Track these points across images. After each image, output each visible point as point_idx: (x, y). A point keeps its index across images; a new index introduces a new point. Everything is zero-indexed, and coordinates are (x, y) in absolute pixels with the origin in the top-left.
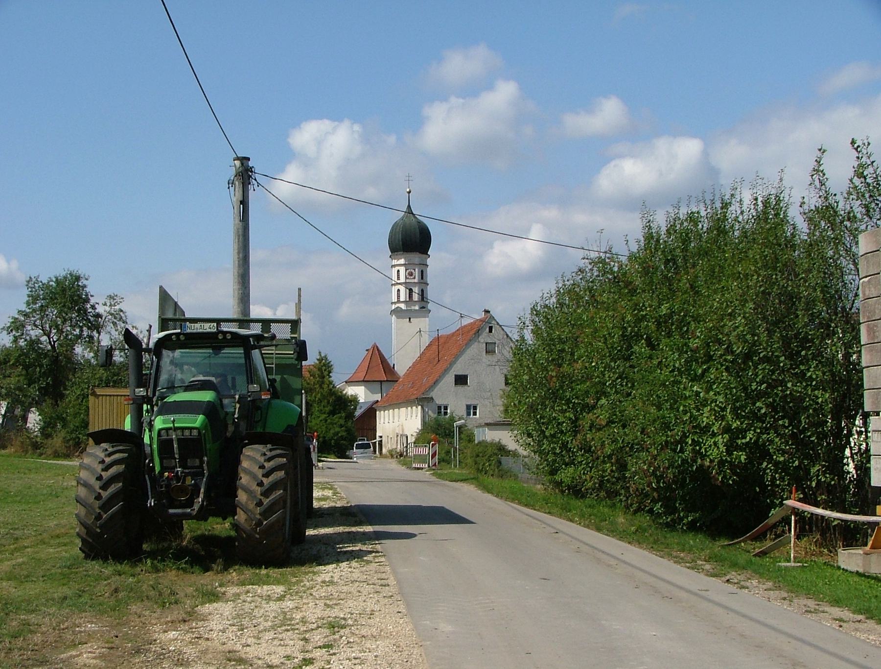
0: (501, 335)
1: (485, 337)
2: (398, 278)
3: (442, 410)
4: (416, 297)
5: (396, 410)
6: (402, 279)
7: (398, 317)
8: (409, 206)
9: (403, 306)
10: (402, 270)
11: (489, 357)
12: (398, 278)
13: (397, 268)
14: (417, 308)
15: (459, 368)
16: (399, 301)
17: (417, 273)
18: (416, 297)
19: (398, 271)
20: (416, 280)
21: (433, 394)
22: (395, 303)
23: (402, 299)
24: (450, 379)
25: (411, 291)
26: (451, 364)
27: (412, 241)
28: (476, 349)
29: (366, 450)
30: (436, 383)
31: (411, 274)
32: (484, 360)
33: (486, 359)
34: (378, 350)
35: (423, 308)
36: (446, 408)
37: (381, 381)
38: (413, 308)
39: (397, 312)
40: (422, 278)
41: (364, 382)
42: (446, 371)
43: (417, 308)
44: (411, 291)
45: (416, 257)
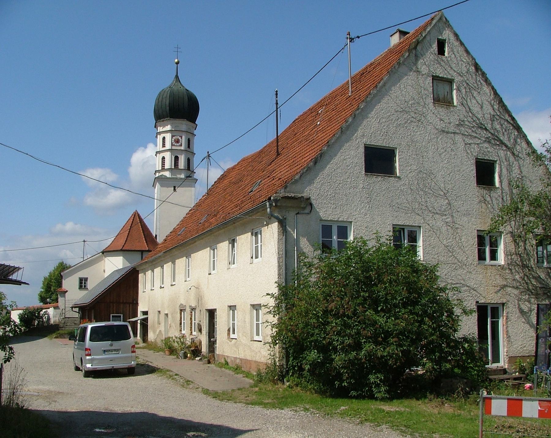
0: (464, 66)
1: (428, 63)
2: (164, 145)
3: (331, 236)
4: (182, 164)
5: (181, 262)
6: (168, 146)
7: (162, 186)
8: (177, 77)
9: (167, 174)
10: (168, 136)
11: (442, 111)
12: (164, 145)
13: (163, 135)
14: (183, 176)
15: (374, 130)
16: (163, 169)
17: (184, 141)
18: (182, 164)
19: (164, 139)
20: (182, 148)
21: (313, 191)
22: (159, 171)
23: (167, 166)
24: (352, 155)
25: (177, 158)
26: (358, 116)
27: (180, 108)
28: (411, 88)
29: (117, 344)
30: (319, 160)
31: (177, 141)
32: (431, 117)
33: (435, 115)
35: (189, 177)
36: (343, 232)
37: (142, 252)
38: (178, 176)
39: (161, 180)
40: (189, 147)
41: (123, 251)
42: (345, 132)
43: (183, 176)
44: (177, 158)
45: (184, 124)
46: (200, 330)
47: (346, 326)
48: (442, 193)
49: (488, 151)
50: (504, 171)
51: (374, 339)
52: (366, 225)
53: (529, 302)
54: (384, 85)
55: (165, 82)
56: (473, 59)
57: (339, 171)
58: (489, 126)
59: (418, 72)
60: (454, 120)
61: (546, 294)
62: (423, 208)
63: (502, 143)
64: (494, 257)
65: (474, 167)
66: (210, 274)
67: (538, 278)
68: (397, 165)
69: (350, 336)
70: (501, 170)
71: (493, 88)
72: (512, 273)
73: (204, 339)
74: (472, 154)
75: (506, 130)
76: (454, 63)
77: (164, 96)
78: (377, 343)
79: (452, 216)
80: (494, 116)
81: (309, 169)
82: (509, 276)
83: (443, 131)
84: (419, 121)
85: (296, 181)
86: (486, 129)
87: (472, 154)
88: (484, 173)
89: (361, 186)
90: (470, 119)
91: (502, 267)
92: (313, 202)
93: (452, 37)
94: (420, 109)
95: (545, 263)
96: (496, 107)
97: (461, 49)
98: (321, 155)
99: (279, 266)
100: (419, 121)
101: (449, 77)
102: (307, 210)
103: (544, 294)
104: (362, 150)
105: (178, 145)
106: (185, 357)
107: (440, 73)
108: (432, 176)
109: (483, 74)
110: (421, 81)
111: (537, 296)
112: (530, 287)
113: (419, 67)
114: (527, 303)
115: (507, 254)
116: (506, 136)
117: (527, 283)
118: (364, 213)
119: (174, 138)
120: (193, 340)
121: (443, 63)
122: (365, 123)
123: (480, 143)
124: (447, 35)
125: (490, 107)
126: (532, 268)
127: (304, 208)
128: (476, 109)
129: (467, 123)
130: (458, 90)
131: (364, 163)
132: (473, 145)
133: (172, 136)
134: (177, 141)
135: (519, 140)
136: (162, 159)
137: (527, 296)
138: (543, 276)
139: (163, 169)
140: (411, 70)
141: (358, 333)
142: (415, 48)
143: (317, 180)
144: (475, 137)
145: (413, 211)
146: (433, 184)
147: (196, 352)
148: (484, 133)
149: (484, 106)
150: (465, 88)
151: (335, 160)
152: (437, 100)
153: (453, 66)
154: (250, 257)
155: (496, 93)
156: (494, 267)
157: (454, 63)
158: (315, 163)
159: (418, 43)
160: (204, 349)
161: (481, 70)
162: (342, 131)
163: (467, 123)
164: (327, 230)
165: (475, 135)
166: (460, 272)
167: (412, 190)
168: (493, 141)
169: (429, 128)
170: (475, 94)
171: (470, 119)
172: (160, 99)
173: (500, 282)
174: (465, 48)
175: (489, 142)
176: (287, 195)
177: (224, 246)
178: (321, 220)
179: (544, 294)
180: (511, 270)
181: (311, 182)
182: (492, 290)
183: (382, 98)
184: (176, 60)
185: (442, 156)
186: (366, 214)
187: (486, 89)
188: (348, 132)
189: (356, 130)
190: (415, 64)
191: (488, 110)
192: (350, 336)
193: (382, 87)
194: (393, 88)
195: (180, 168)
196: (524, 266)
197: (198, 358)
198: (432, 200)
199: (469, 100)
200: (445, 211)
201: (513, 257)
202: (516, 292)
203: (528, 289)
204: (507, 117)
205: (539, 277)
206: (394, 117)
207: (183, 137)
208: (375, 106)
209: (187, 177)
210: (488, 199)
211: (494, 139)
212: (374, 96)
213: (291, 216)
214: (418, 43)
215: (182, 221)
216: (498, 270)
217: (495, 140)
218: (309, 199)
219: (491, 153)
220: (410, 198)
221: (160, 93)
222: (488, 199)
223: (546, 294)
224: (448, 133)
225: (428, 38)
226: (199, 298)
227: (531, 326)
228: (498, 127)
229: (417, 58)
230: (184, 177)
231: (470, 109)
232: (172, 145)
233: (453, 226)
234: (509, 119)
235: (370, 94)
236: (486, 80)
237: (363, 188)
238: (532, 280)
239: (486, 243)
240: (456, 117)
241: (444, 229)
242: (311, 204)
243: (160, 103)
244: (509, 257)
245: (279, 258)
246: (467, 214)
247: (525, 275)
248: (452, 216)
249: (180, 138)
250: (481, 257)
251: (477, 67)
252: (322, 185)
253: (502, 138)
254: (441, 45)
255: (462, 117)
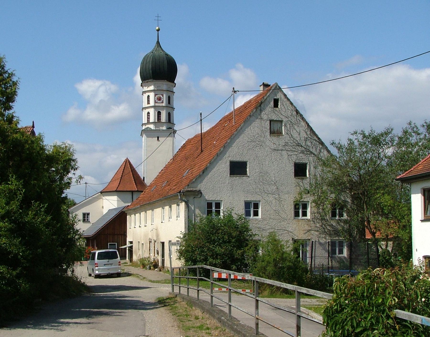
0: (289, 111)
1: (269, 112)
2: (148, 103)
3: (213, 207)
4: (164, 118)
5: (149, 212)
6: (152, 103)
7: (148, 136)
8: (158, 43)
9: (152, 127)
10: (152, 95)
11: (275, 139)
12: (148, 103)
13: (147, 94)
14: (164, 128)
15: (235, 153)
16: (148, 122)
17: (165, 98)
18: (164, 118)
19: (148, 97)
20: (164, 104)
21: (201, 186)
22: (145, 124)
23: (152, 120)
24: (223, 167)
25: (159, 113)
26: (226, 147)
27: (161, 71)
28: (258, 128)
29: (111, 261)
30: (205, 171)
31: (159, 99)
32: (268, 143)
33: (271, 142)
34: (129, 161)
35: (170, 128)
36: (218, 205)
37: (132, 192)
38: (161, 128)
39: (147, 132)
40: (169, 103)
41: (117, 192)
42: (219, 156)
43: (164, 128)
44: (159, 113)
45: (164, 85)
46: (158, 254)
47: (202, 251)
48: (273, 183)
49: (302, 158)
50: (312, 168)
51: (212, 256)
52: (230, 202)
53: (325, 238)
54: (241, 128)
55: (147, 48)
56: (295, 107)
57: (216, 175)
58: (303, 144)
59: (261, 119)
60: (282, 142)
61: (336, 234)
62: (262, 191)
63: (312, 153)
64: (305, 214)
65: (293, 168)
66: (162, 222)
67: (331, 226)
68: (248, 170)
69: (203, 255)
70: (310, 168)
71: (307, 123)
72: (315, 223)
73: (160, 258)
74: (292, 161)
75: (314, 145)
76: (283, 112)
77: (148, 60)
78: (213, 259)
79: (279, 195)
80: (307, 138)
81: (200, 176)
82: (313, 225)
83: (275, 150)
84: (261, 145)
85: (194, 182)
86: (301, 146)
87: (292, 161)
88: (300, 170)
89: (228, 182)
90: (292, 142)
91: (309, 220)
92: (202, 192)
93: (283, 97)
94: (262, 139)
95: (337, 217)
96: (308, 133)
97: (288, 103)
98: (206, 168)
99: (185, 223)
100: (261, 145)
101: (280, 119)
102: (199, 196)
103: (335, 234)
104: (228, 164)
105: (160, 102)
106: (150, 269)
107: (274, 118)
108: (268, 174)
109: (301, 115)
110: (263, 124)
111: (330, 235)
112: (326, 231)
113: (262, 116)
114: (323, 239)
115: (311, 213)
116: (314, 149)
117: (324, 228)
118: (229, 196)
119: (157, 96)
120: (154, 260)
121: (276, 112)
122: (230, 149)
123: (298, 154)
124: (279, 96)
125: (304, 133)
126: (328, 220)
127: (197, 195)
128: (295, 135)
129: (290, 144)
130: (285, 126)
131: (229, 171)
132: (293, 156)
133: (155, 95)
134: (159, 99)
135: (322, 150)
136: (148, 114)
137: (324, 235)
138: (334, 224)
139: (148, 122)
140: (257, 119)
141: (207, 254)
142: (260, 106)
143: (205, 181)
144: (295, 151)
145: (256, 193)
146: (268, 178)
147: (156, 266)
148: (300, 149)
149: (301, 133)
150: (290, 124)
151: (214, 170)
152: (272, 133)
153: (283, 113)
154: (176, 216)
155: (308, 125)
156: (303, 221)
157: (283, 112)
158: (203, 173)
159: (262, 103)
160: (160, 264)
161: (300, 113)
162: (217, 156)
163: (290, 144)
164: (209, 205)
165: (294, 150)
166: (283, 223)
167: (255, 182)
168: (305, 152)
169: (267, 149)
170: (296, 127)
171: (292, 142)
172: (145, 63)
173: (307, 228)
174: (290, 101)
175: (303, 153)
176: (189, 189)
177: (167, 208)
178: (206, 200)
179: (335, 234)
180: (314, 221)
181: (201, 182)
182: (302, 232)
183: (240, 136)
184: (157, 28)
185: (274, 163)
186: (230, 196)
187: (303, 123)
188: (221, 156)
189: (226, 154)
190: (260, 114)
191: (303, 135)
192: (203, 255)
193: (240, 130)
194: (246, 130)
195: (162, 121)
196: (322, 219)
197: (156, 269)
198: (267, 187)
199: (291, 131)
200: (275, 192)
201: (315, 215)
202: (317, 233)
203: (325, 232)
204: (315, 138)
205: (332, 225)
206: (247, 145)
207: (164, 95)
208: (236, 140)
209: (168, 129)
210: (301, 184)
211: (307, 151)
212: (235, 135)
213: (191, 199)
214: (262, 103)
215: (156, 178)
216: (306, 222)
217: (307, 151)
218: (200, 190)
219: (303, 159)
220: (254, 186)
221: (144, 58)
222: (301, 184)
223: (336, 234)
224: (278, 150)
225: (268, 99)
226: (158, 235)
227: (326, 251)
228: (309, 144)
229: (261, 111)
230: (165, 129)
231: (292, 136)
232: (155, 102)
233: (279, 200)
234: (317, 139)
235: (233, 134)
236: (303, 119)
237: (229, 183)
238: (327, 226)
239: (300, 208)
240: (283, 141)
241: (274, 201)
242: (201, 193)
243: (144, 67)
244: (313, 215)
245: (185, 219)
246: (288, 193)
247: (322, 224)
248: (279, 195)
249: (162, 96)
250: (297, 214)
251: (297, 112)
252: (207, 183)
253: (311, 150)
254: (276, 102)
255: (287, 141)
